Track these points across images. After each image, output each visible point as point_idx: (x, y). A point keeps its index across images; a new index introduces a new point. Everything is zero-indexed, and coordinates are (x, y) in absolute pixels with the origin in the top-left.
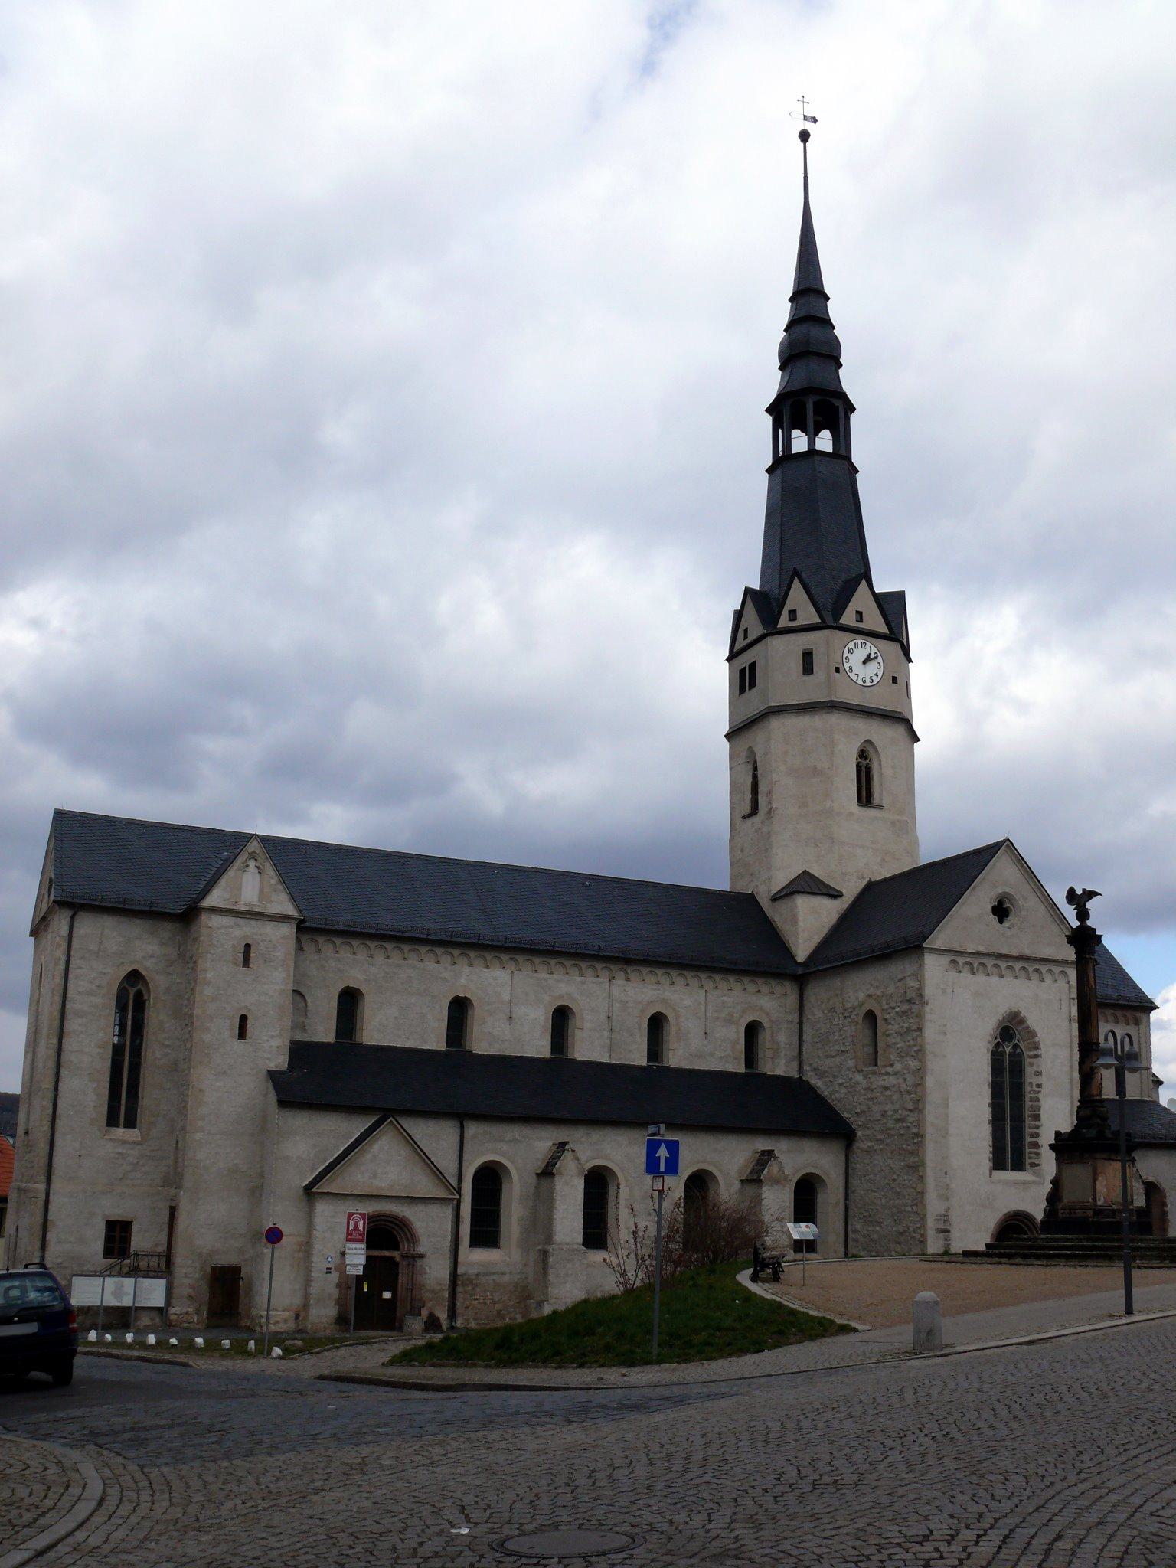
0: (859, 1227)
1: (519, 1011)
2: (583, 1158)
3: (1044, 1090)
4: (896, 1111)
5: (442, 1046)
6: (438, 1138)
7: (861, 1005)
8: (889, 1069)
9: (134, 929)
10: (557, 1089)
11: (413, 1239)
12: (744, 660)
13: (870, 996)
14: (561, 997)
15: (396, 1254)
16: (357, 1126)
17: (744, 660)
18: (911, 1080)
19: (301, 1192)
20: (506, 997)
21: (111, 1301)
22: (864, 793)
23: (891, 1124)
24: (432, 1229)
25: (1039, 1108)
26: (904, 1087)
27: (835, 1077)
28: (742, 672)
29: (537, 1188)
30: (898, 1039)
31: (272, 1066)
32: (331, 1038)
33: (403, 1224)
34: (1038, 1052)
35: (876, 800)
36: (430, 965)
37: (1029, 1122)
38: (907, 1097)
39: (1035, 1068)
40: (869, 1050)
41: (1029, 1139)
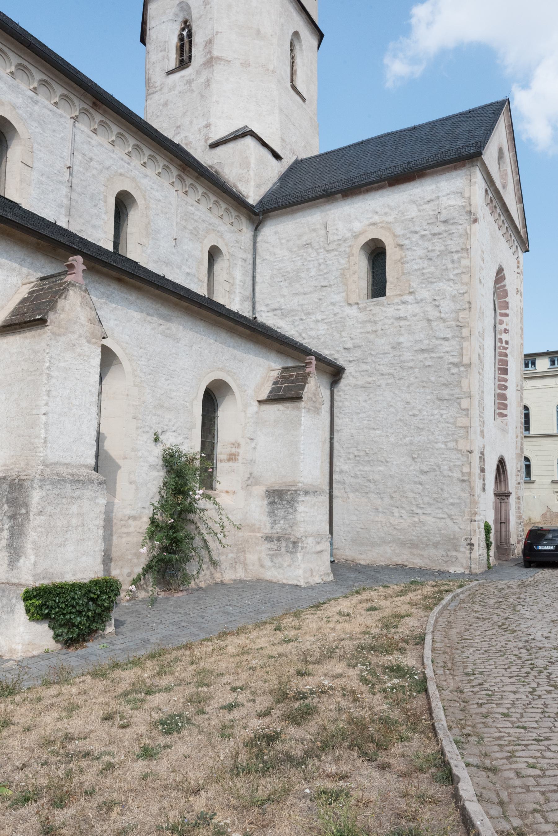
0: (345, 467)
4: (416, 342)
8: (409, 298)
13: (374, 224)
18: (447, 306)
23: (407, 355)
25: (506, 363)
26: (433, 313)
27: (309, 314)
30: (426, 264)
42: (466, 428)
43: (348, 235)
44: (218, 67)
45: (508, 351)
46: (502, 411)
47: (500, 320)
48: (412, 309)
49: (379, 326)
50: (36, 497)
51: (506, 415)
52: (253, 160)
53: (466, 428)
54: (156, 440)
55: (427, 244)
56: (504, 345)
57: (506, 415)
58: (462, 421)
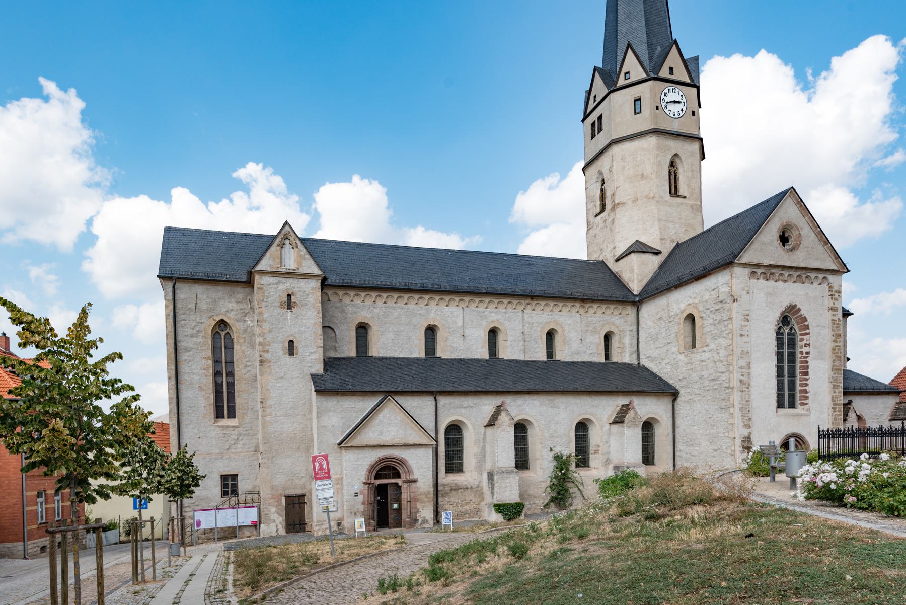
1: (468, 332)
2: (513, 415)
3: (811, 356)
5: (423, 355)
6: (422, 406)
7: (682, 312)
8: (706, 349)
9: (218, 292)
10: (494, 377)
11: (409, 471)
12: (594, 117)
14: (493, 322)
15: (399, 481)
16: (369, 403)
17: (594, 117)
19: (336, 447)
20: (460, 323)
21: (220, 525)
22: (673, 187)
24: (420, 466)
25: (808, 367)
28: (593, 124)
29: (485, 435)
31: (313, 371)
32: (353, 353)
33: (402, 462)
35: (682, 190)
36: (412, 305)
37: (799, 377)
38: (719, 365)
40: (689, 339)
42: (733, 424)
43: (679, 311)
44: (618, 210)
48: (708, 355)
49: (693, 366)
50: (495, 478)
52: (635, 267)
53: (733, 424)
54: (551, 450)
55: (712, 316)
58: (731, 421)
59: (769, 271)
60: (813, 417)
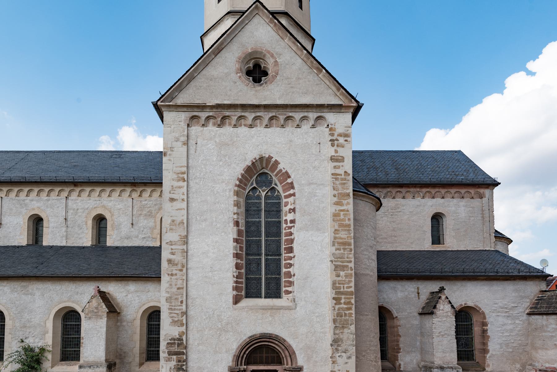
3: (296, 225)
34: (292, 192)
37: (284, 255)
39: (289, 207)
41: (284, 270)
45: (292, 230)
46: (287, 289)
47: (285, 202)
51: (290, 292)
56: (289, 225)
57: (290, 292)
59: (223, 113)
60: (300, 312)
